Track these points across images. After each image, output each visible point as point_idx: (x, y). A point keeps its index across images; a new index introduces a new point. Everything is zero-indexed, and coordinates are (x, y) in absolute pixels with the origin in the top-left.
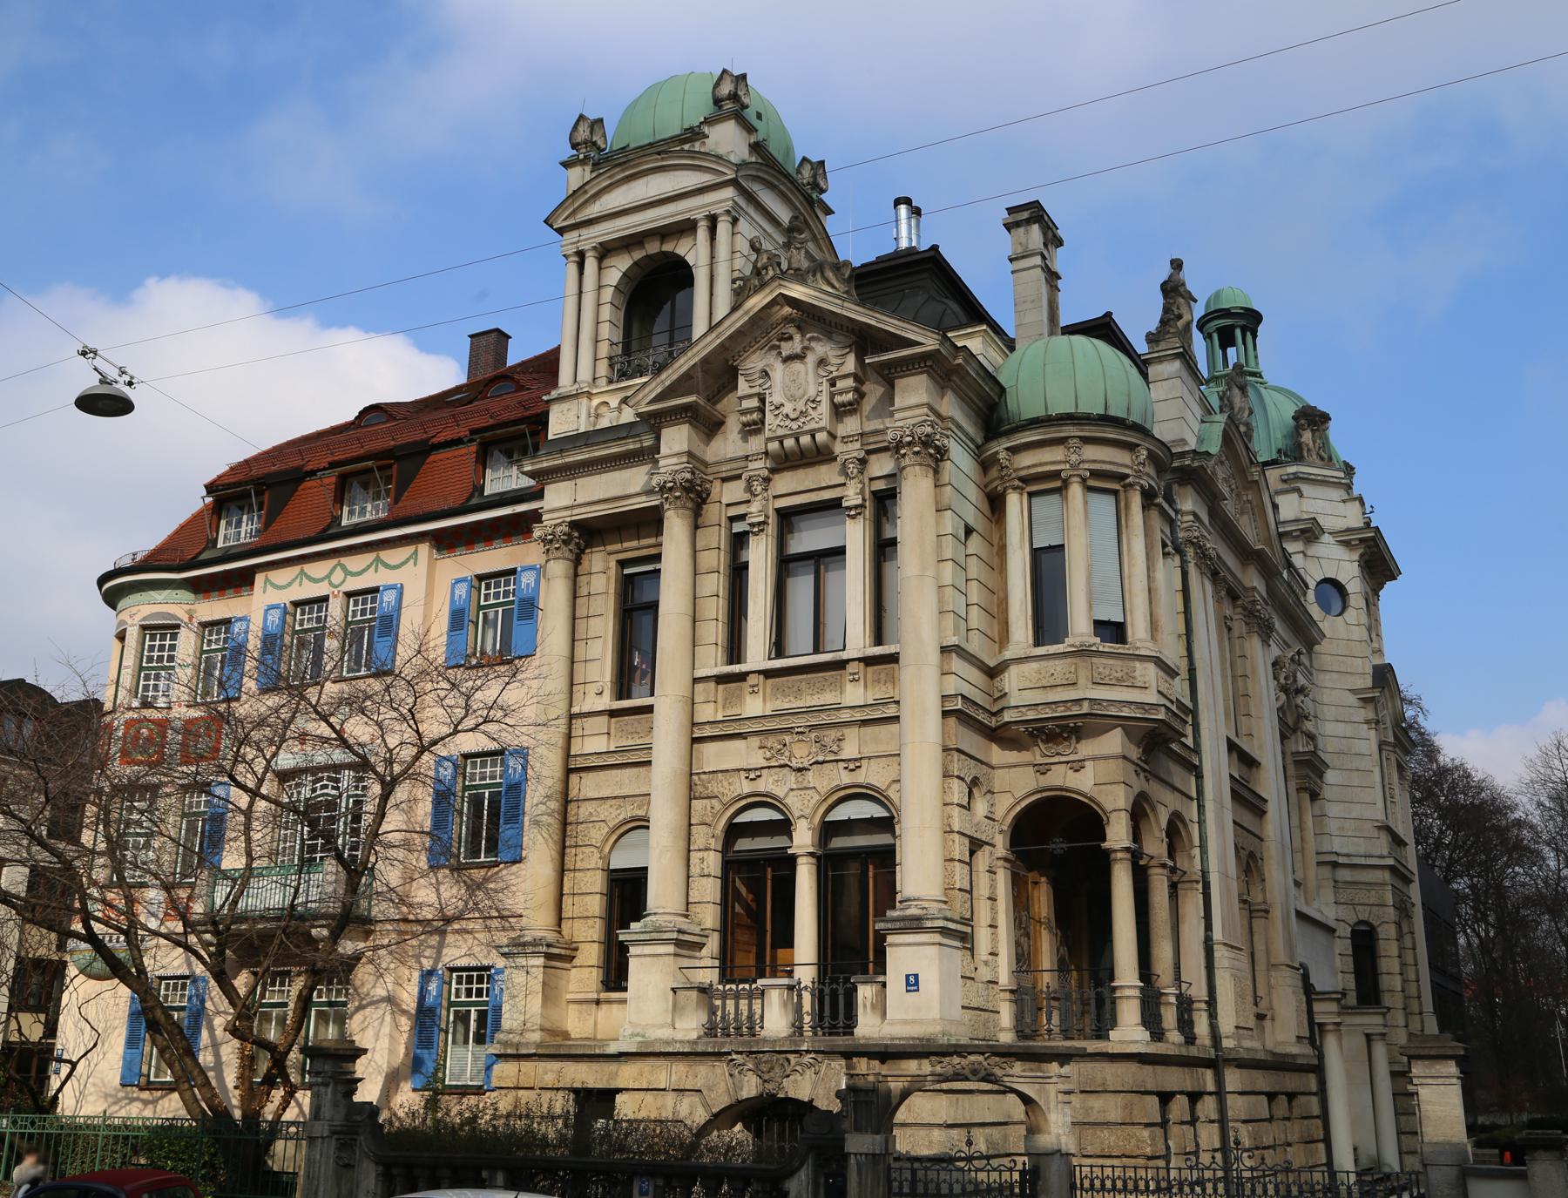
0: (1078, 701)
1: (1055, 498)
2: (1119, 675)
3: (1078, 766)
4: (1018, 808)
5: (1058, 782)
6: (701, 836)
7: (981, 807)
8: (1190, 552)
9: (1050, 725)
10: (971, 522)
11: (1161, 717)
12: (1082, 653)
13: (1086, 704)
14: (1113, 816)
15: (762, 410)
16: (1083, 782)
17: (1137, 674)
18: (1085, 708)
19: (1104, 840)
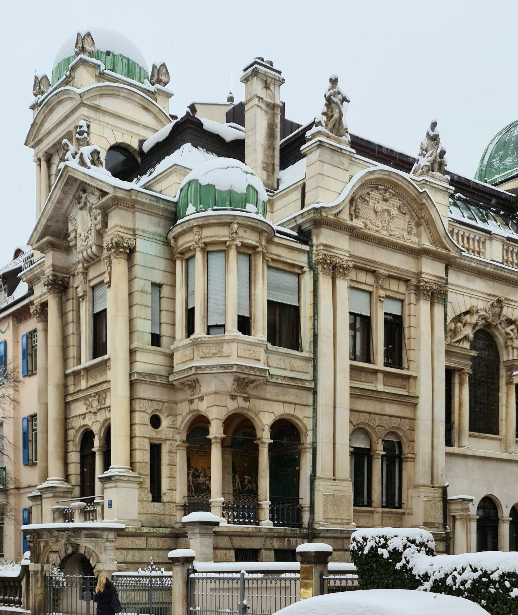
0: (191, 368)
1: (222, 255)
2: (214, 352)
3: (201, 399)
4: (185, 422)
5: (196, 408)
6: (71, 447)
7: (165, 422)
8: (320, 267)
9: (185, 379)
10: (158, 280)
11: (234, 369)
12: (196, 344)
13: (193, 369)
14: (212, 422)
15: (75, 238)
16: (202, 407)
17: (224, 350)
18: (193, 371)
19: (208, 434)
